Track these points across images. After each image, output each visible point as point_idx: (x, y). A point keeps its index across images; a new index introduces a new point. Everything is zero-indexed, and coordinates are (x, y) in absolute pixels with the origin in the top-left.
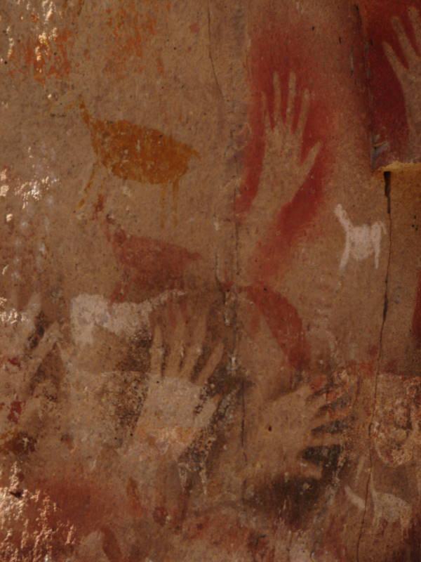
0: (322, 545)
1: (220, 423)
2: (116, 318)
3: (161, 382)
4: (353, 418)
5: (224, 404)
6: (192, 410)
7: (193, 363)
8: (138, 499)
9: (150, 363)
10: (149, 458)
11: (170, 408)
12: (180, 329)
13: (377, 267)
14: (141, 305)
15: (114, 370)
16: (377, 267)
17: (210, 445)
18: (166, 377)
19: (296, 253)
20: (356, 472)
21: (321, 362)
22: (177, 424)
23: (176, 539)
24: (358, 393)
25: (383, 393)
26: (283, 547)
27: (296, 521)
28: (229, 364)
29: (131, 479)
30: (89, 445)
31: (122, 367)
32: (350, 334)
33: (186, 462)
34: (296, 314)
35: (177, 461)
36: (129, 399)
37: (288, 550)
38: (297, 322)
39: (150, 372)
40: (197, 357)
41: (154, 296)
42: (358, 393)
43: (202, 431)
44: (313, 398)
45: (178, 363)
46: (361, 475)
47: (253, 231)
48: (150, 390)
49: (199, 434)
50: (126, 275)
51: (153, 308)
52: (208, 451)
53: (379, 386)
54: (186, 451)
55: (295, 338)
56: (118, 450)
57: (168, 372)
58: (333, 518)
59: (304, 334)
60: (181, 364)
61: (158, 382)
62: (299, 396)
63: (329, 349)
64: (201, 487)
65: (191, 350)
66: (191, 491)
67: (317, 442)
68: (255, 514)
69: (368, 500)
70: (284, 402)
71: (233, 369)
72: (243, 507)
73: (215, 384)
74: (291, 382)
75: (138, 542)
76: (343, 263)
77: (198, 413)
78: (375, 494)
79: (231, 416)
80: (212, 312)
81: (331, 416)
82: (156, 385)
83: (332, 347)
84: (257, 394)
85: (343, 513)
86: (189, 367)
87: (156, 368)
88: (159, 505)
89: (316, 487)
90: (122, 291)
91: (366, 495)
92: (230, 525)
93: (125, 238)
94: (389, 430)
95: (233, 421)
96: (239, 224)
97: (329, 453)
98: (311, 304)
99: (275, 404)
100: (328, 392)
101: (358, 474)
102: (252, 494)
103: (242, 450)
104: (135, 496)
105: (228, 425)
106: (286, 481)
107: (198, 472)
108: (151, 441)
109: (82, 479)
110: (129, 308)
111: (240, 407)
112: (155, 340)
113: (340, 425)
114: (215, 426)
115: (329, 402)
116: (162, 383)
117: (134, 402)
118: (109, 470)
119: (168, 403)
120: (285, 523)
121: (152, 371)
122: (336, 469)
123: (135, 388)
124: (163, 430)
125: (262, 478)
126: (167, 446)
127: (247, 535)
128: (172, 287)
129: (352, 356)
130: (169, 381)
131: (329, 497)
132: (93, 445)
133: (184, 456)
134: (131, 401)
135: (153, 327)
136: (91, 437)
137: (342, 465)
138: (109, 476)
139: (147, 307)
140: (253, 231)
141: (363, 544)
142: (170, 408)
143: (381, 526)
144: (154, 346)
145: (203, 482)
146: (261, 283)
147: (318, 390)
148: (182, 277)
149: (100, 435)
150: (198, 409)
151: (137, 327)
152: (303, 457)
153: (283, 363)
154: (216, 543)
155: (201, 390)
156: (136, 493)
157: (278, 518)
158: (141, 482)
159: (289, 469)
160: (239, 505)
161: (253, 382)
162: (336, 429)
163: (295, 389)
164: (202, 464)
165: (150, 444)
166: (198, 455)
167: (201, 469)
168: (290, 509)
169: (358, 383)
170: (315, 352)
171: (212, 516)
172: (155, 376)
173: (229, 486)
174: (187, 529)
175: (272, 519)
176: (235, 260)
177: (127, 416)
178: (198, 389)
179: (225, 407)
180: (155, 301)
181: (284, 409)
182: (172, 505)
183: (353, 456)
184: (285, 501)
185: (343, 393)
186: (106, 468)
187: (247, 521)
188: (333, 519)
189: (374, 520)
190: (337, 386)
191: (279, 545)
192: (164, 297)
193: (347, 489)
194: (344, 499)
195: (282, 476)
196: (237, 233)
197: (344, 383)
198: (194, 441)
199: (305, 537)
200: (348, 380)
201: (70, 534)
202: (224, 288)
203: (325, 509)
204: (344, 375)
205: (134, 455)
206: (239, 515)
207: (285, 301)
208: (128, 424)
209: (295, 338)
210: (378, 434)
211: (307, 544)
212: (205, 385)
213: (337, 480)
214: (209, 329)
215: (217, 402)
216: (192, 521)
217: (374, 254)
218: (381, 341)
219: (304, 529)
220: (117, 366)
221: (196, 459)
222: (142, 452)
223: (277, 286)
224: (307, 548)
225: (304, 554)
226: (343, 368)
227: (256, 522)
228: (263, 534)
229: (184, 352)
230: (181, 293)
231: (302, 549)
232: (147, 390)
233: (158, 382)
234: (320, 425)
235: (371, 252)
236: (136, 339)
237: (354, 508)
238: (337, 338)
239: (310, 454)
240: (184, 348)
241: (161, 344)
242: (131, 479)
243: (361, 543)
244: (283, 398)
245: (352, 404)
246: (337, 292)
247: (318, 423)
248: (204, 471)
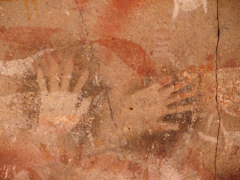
0: (183, 164)
1: (95, 110)
2: (9, 68)
3: (48, 95)
4: (200, 95)
5: (96, 100)
6: (74, 106)
7: (68, 83)
8: (48, 153)
9: (39, 87)
10: (51, 132)
11: (59, 107)
12: (55, 67)
13: (206, 12)
14: (25, 60)
15: (16, 93)
16: (206, 12)
17: (91, 122)
18: (52, 92)
19: (133, 17)
20: (207, 123)
21: (165, 70)
22: (65, 114)
23: (78, 170)
24: (200, 82)
25: (223, 79)
26: (155, 168)
27: (162, 153)
28: (94, 80)
29: (41, 144)
30: (10, 130)
31: (21, 91)
32: (188, 51)
33: (76, 132)
34: (140, 48)
35: (70, 131)
36: (30, 106)
37: (159, 169)
38: (141, 51)
39: (40, 91)
40: (69, 80)
41: (33, 54)
42: (200, 82)
43: (83, 115)
44: (163, 89)
45: (58, 84)
46: (212, 124)
47: (94, 12)
48: (42, 99)
49: (83, 117)
50: (11, 47)
51: (34, 60)
52: (92, 124)
53: (218, 76)
54: (76, 126)
55: (141, 60)
56: (30, 130)
57: (52, 89)
58: (191, 151)
59: (149, 57)
60: (60, 85)
61: (47, 95)
62: (152, 90)
63: (170, 63)
64: (90, 143)
65: (64, 77)
66: (83, 145)
67: (172, 111)
68: (130, 153)
69: (220, 137)
70: (140, 94)
71: (97, 82)
72: (120, 150)
73: (87, 91)
74: (143, 83)
75: (52, 173)
76: (175, 15)
77: (79, 107)
78: (226, 133)
79: (101, 106)
80: (77, 56)
81: (181, 96)
82: (46, 96)
83: (173, 61)
84: (116, 94)
85: (198, 146)
86: (66, 84)
87: (44, 89)
88: (62, 155)
89: (174, 136)
90: (11, 55)
91: (218, 134)
92: (113, 161)
93: (6, 29)
94: (234, 98)
95: (103, 108)
96: (81, 10)
97: (183, 116)
98: (152, 41)
99: (133, 96)
100: (175, 85)
101: (209, 124)
102: (126, 143)
103: (112, 123)
104: (46, 151)
105: (100, 111)
106: (151, 134)
107: (86, 136)
108: (51, 124)
109: (10, 147)
110: (17, 62)
111: (106, 100)
112: (38, 75)
113: (189, 100)
114: (92, 112)
115: (177, 90)
116: (50, 95)
117: (34, 106)
118: (26, 141)
119: (57, 104)
120: (154, 155)
121: (41, 90)
122: (190, 123)
123: (32, 100)
124: (57, 118)
125: (132, 134)
126: (62, 125)
127: (126, 164)
128: (45, 48)
129: (191, 63)
130: (54, 94)
131: (186, 139)
132: (12, 130)
133: (76, 128)
134: (32, 106)
135: (36, 69)
136: (11, 126)
137: (195, 121)
138: (26, 143)
139: (29, 61)
140: (94, 12)
141: (219, 161)
142: (59, 107)
143: (234, 150)
144: (38, 78)
145: (91, 140)
146: (109, 36)
147: (165, 85)
148: (50, 42)
149: (17, 125)
150: (78, 106)
151: (23, 71)
152: (162, 120)
153: (133, 75)
154: (105, 170)
155: (78, 96)
156: (46, 150)
157: (149, 153)
158: (49, 144)
159: (152, 128)
160: (118, 149)
161: (112, 87)
162: (186, 103)
163: (147, 86)
164: (88, 132)
165: (50, 125)
166: (85, 127)
167: (87, 134)
168: (158, 147)
169: (200, 77)
170: (158, 67)
171: (100, 157)
172: (44, 92)
173: (110, 140)
174: (84, 164)
175: (144, 154)
176: (84, 28)
177: (32, 114)
178: (76, 95)
179: (96, 102)
180: (35, 56)
181: (142, 97)
182: (71, 154)
183: (203, 115)
184: (153, 144)
185: (188, 83)
186: (23, 140)
187: (124, 157)
188: (191, 151)
189: (226, 148)
190: (181, 81)
191: (150, 167)
192: (41, 53)
193: (200, 134)
194: (198, 139)
195: (147, 132)
196: (81, 15)
197: (186, 78)
198: (80, 121)
199: (171, 161)
200: (189, 76)
201: (7, 173)
202: (83, 42)
203: (184, 145)
204: (185, 74)
205: (41, 132)
206: (118, 155)
207: (131, 42)
208: (34, 117)
209: (141, 60)
210: (224, 101)
211: (172, 165)
212: (80, 92)
213: (191, 129)
214: (75, 65)
215: (90, 100)
216: (85, 161)
217: (202, 6)
218: (216, 51)
219: (170, 157)
220: (17, 91)
221: (84, 130)
222: (46, 130)
223: (121, 36)
224: (173, 167)
225: (171, 170)
226: (184, 71)
227: (132, 157)
228: (138, 162)
229: (60, 79)
230: (52, 50)
231: (169, 167)
232: (40, 100)
233: (47, 95)
234: (173, 102)
235: (200, 5)
236: (25, 76)
237: (206, 143)
238: (176, 56)
239: (167, 118)
240: (60, 77)
241: (43, 77)
242: (41, 144)
243: (217, 161)
244: (139, 92)
245: (196, 88)
246: (173, 31)
247: (172, 101)
248: (91, 135)
